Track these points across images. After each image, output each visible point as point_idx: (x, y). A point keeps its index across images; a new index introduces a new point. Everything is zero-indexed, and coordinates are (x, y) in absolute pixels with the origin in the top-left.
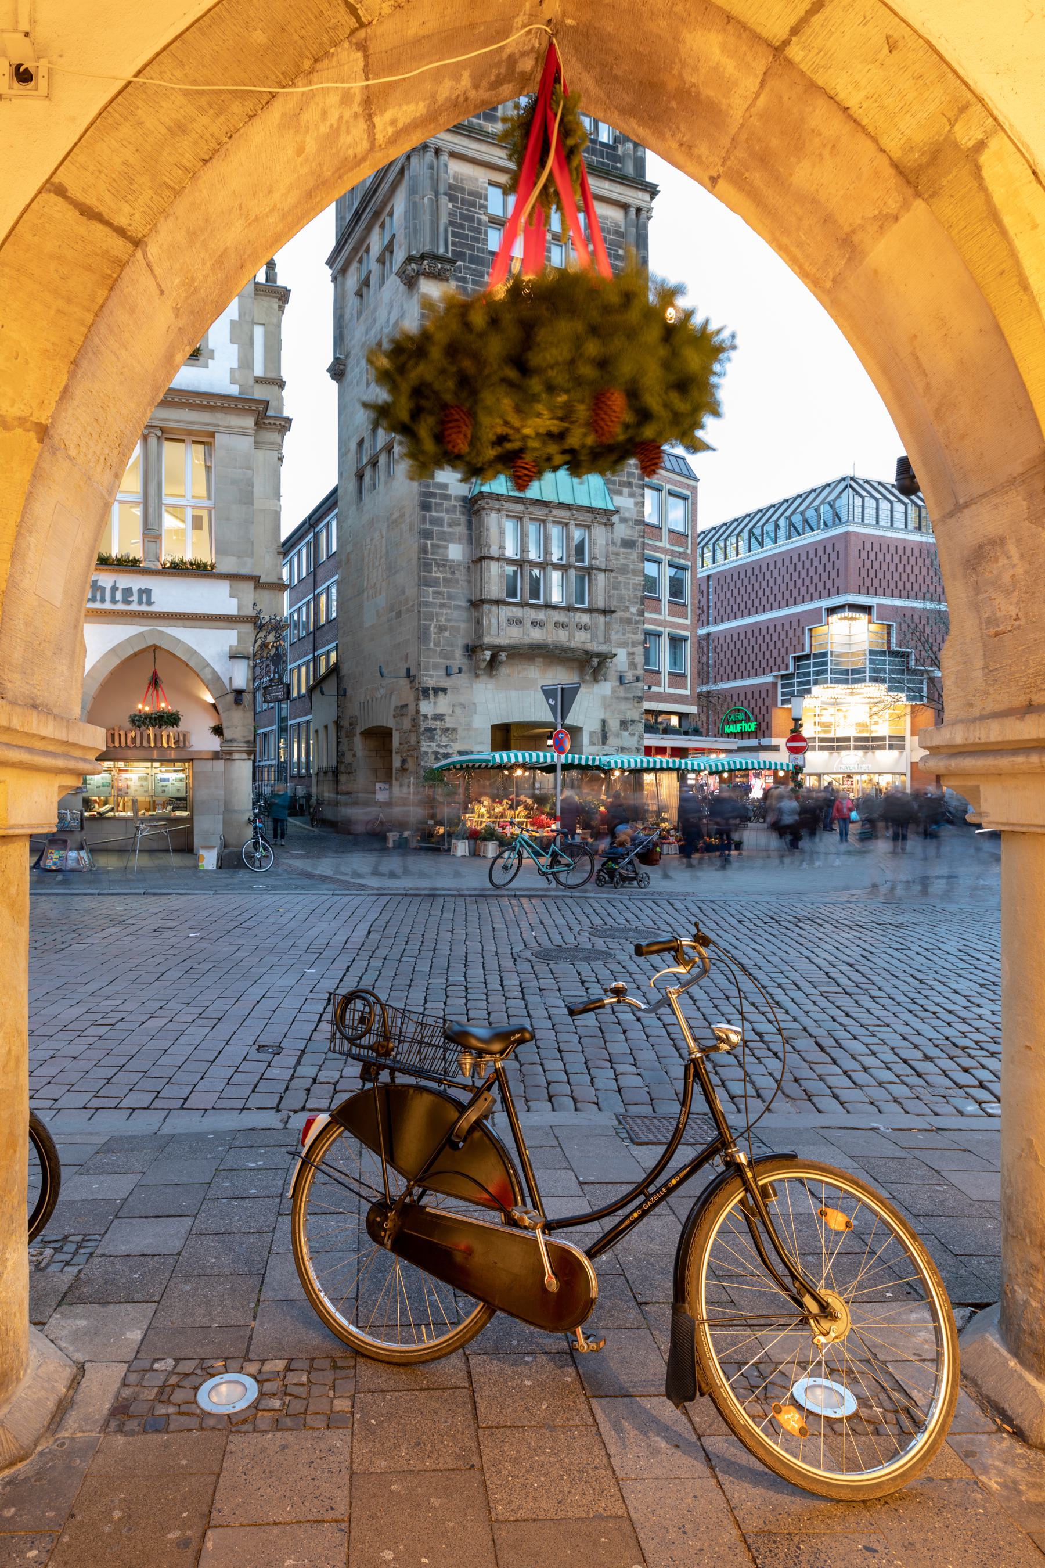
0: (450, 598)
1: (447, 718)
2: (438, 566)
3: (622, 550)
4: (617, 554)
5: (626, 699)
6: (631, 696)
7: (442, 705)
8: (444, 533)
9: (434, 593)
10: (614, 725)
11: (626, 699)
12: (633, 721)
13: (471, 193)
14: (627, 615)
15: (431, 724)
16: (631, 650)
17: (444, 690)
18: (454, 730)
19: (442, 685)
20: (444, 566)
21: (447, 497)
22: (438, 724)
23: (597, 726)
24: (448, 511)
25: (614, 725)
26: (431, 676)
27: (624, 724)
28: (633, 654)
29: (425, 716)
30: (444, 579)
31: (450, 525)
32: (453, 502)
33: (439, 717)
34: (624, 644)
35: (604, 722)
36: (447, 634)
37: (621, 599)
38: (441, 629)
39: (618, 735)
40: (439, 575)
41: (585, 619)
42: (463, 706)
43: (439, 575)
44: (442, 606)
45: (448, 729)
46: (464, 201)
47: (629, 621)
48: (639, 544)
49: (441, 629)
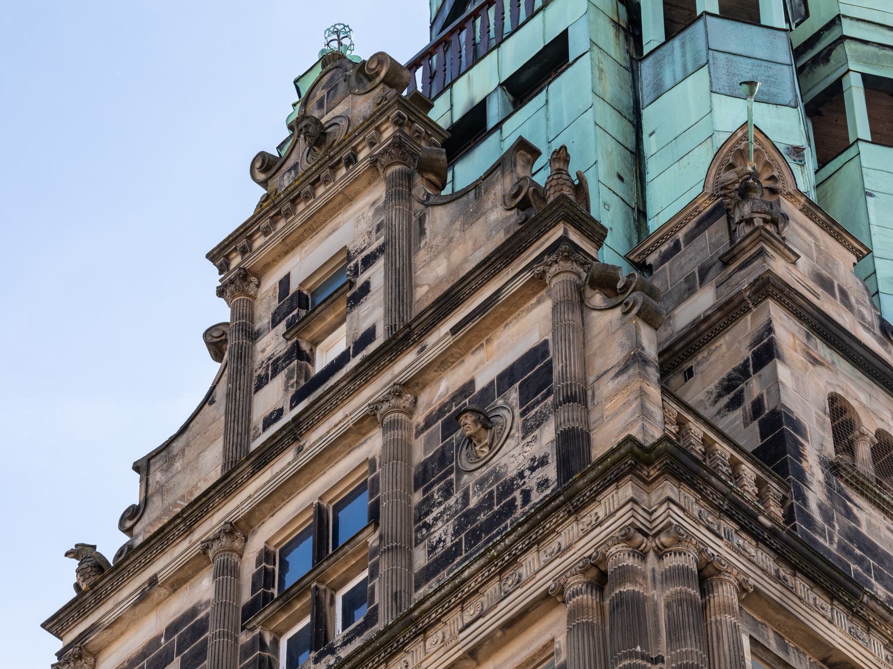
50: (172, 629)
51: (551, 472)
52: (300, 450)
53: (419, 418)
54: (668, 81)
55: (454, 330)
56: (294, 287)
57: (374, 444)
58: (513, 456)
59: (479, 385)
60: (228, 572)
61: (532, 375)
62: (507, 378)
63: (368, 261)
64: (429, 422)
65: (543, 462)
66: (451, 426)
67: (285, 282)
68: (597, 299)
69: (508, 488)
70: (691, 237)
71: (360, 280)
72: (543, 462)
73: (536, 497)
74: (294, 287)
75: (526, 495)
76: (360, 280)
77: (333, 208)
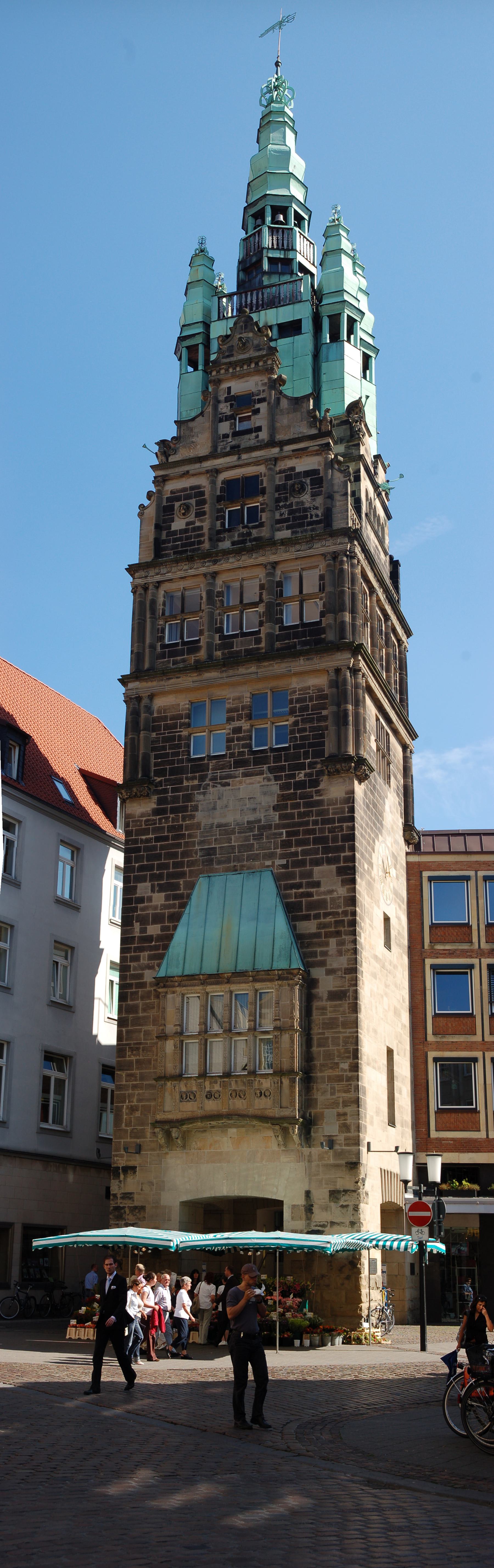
0: (142, 1078)
1: (136, 1196)
2: (132, 1050)
3: (329, 1003)
4: (324, 1008)
5: (337, 1166)
6: (343, 1162)
7: (130, 1184)
8: (139, 1018)
9: (127, 1075)
10: (320, 1196)
11: (337, 1166)
12: (346, 1191)
13: (173, 718)
14: (337, 1073)
15: (120, 1203)
16: (341, 1110)
17: (133, 1169)
18: (142, 1208)
19: (131, 1164)
20: (138, 1049)
21: (143, 985)
22: (127, 1203)
23: (301, 1201)
24: (143, 998)
25: (320, 1196)
26: (122, 1156)
27: (334, 1194)
28: (345, 1114)
29: (115, 1195)
30: (138, 1061)
31: (144, 1010)
32: (148, 989)
33: (128, 1196)
34: (335, 1104)
35: (308, 1194)
36: (138, 1114)
37: (329, 1055)
38: (133, 1109)
39: (326, 1208)
40: (133, 1058)
41: (266, 1084)
42: (151, 1183)
43: (133, 1058)
44: (135, 1087)
45: (136, 1208)
46: (167, 727)
47: (339, 1079)
48: (351, 994)
49: (133, 1109)
50: (192, 488)
51: (319, 513)
52: (239, 458)
53: (278, 469)
54: (331, 358)
55: (293, 451)
56: (232, 393)
57: (262, 469)
58: (306, 498)
59: (297, 470)
60: (213, 483)
61: (316, 478)
62: (307, 473)
63: (261, 401)
64: (281, 472)
65: (317, 508)
66: (288, 478)
67: (229, 388)
68: (336, 466)
69: (306, 510)
70: (339, 425)
71: (257, 406)
72: (317, 508)
73: (314, 519)
74: (232, 393)
75: (311, 517)
76: (257, 406)
77: (249, 374)
